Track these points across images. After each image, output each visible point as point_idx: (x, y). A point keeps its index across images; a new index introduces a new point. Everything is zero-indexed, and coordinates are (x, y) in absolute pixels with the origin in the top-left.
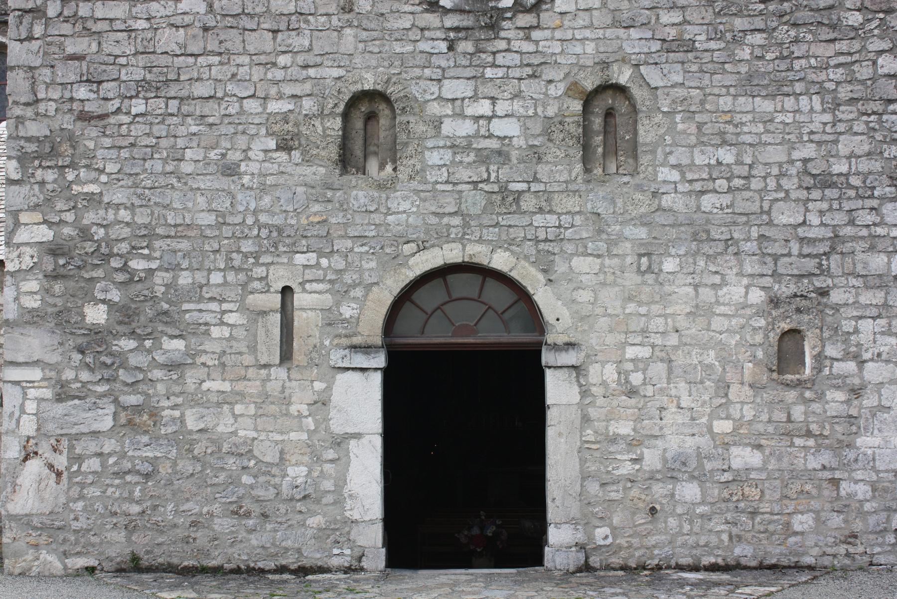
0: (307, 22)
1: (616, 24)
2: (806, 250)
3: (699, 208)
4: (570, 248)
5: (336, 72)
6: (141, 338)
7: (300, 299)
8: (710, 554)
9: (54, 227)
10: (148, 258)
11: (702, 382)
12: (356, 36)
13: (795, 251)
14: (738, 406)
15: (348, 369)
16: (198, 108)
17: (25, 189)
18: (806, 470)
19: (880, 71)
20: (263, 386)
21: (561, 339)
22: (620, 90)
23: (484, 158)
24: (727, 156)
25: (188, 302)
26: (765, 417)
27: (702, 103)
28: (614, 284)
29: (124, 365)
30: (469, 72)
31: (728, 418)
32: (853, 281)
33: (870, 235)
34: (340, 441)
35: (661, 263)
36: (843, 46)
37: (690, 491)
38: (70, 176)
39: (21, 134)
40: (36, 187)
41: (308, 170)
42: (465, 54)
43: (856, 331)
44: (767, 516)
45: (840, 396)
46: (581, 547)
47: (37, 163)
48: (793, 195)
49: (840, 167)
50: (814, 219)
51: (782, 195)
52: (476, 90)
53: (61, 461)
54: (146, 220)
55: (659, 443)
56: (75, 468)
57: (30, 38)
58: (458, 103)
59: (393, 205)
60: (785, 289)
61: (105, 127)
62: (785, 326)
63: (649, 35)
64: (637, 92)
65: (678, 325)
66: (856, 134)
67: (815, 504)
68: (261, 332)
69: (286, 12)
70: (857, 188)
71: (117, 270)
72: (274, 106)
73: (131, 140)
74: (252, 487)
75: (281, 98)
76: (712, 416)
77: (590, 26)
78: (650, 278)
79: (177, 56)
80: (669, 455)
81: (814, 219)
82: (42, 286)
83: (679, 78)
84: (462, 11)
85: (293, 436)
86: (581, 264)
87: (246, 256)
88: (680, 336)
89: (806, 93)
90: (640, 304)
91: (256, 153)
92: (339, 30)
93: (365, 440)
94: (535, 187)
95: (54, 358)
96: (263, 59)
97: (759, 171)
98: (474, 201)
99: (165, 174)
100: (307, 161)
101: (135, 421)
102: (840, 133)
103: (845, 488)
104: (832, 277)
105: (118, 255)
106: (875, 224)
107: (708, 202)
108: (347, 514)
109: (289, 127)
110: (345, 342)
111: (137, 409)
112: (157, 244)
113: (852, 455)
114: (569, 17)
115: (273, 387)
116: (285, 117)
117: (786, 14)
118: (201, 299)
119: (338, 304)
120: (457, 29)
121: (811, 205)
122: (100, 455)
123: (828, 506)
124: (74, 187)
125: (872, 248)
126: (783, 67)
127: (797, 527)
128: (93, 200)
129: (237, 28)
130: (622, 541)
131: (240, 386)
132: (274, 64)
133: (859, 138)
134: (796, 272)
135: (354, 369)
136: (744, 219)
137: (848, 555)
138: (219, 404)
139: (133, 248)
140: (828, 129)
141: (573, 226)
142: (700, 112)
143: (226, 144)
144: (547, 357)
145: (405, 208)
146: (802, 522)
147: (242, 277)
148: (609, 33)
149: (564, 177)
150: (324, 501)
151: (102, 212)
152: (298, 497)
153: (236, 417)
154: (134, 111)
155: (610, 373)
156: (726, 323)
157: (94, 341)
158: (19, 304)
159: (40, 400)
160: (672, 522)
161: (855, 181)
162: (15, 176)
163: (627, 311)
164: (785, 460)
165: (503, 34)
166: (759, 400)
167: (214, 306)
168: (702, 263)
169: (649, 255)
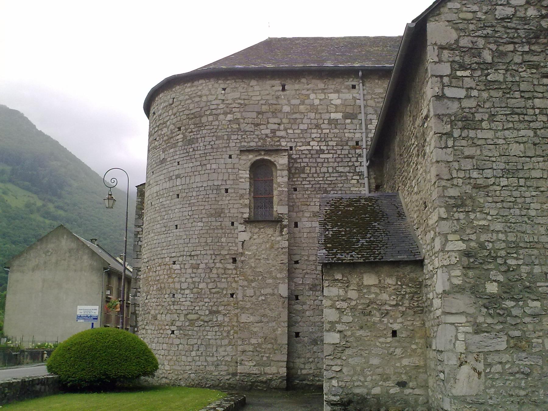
6: (517, 300)
9: (466, 242)
10: (517, 259)
16: (535, 183)
25: (540, 282)
29: (510, 315)
38: (472, 216)
40: (455, 222)
47: (455, 209)
53: (480, 367)
56: (488, 370)
57: (446, 147)
73: (502, 198)
79: (521, 157)
95: (471, 310)
101: (518, 345)
105: (500, 257)
122: (500, 363)
128: (485, 229)
139: (508, 253)
151: (490, 235)
154: (502, 184)
157: (492, 303)
158: (451, 282)
162: (445, 216)
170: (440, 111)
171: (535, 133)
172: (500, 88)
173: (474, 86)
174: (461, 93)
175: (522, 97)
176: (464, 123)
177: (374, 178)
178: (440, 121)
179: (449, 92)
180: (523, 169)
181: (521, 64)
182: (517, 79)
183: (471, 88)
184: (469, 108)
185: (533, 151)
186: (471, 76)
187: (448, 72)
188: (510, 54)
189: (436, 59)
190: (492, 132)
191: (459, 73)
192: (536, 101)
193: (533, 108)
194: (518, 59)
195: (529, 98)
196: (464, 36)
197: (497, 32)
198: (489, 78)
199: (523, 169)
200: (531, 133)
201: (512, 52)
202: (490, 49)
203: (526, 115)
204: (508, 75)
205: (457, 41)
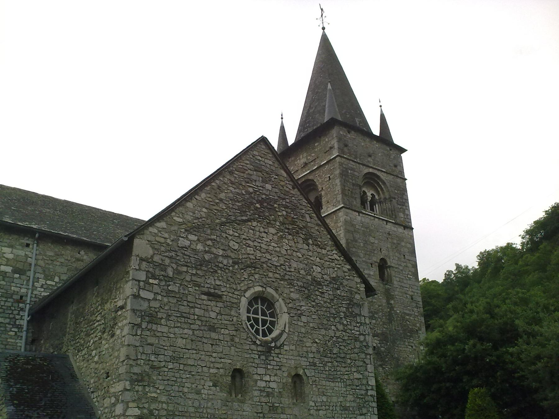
0: (221, 343)
1: (299, 356)
5: (230, 361)
16: (188, 368)
24: (325, 399)
27: (319, 382)
36: (347, 369)
40: (135, 393)
47: (136, 383)
49: (348, 405)
54: (172, 409)
57: (136, 335)
64: (304, 378)
72: (212, 371)
73: (168, 378)
83: (313, 374)
84: (262, 346)
96: (209, 354)
98: (266, 409)
100: (221, 391)
109: (216, 378)
116: (215, 375)
128: (155, 400)
132: (212, 356)
148: (297, 358)
149: (288, 403)
151: (157, 404)
161: (351, 409)
165: (272, 355)
171: (193, 332)
173: (159, 292)
174: (150, 296)
175: (188, 305)
177: (32, 332)
179: (143, 294)
182: (187, 292)
183: (157, 293)
186: (158, 285)
187: (144, 278)
188: (184, 273)
189: (137, 267)
191: (151, 281)
194: (188, 278)
195: (192, 307)
198: (169, 288)
204: (181, 288)
205: (152, 257)
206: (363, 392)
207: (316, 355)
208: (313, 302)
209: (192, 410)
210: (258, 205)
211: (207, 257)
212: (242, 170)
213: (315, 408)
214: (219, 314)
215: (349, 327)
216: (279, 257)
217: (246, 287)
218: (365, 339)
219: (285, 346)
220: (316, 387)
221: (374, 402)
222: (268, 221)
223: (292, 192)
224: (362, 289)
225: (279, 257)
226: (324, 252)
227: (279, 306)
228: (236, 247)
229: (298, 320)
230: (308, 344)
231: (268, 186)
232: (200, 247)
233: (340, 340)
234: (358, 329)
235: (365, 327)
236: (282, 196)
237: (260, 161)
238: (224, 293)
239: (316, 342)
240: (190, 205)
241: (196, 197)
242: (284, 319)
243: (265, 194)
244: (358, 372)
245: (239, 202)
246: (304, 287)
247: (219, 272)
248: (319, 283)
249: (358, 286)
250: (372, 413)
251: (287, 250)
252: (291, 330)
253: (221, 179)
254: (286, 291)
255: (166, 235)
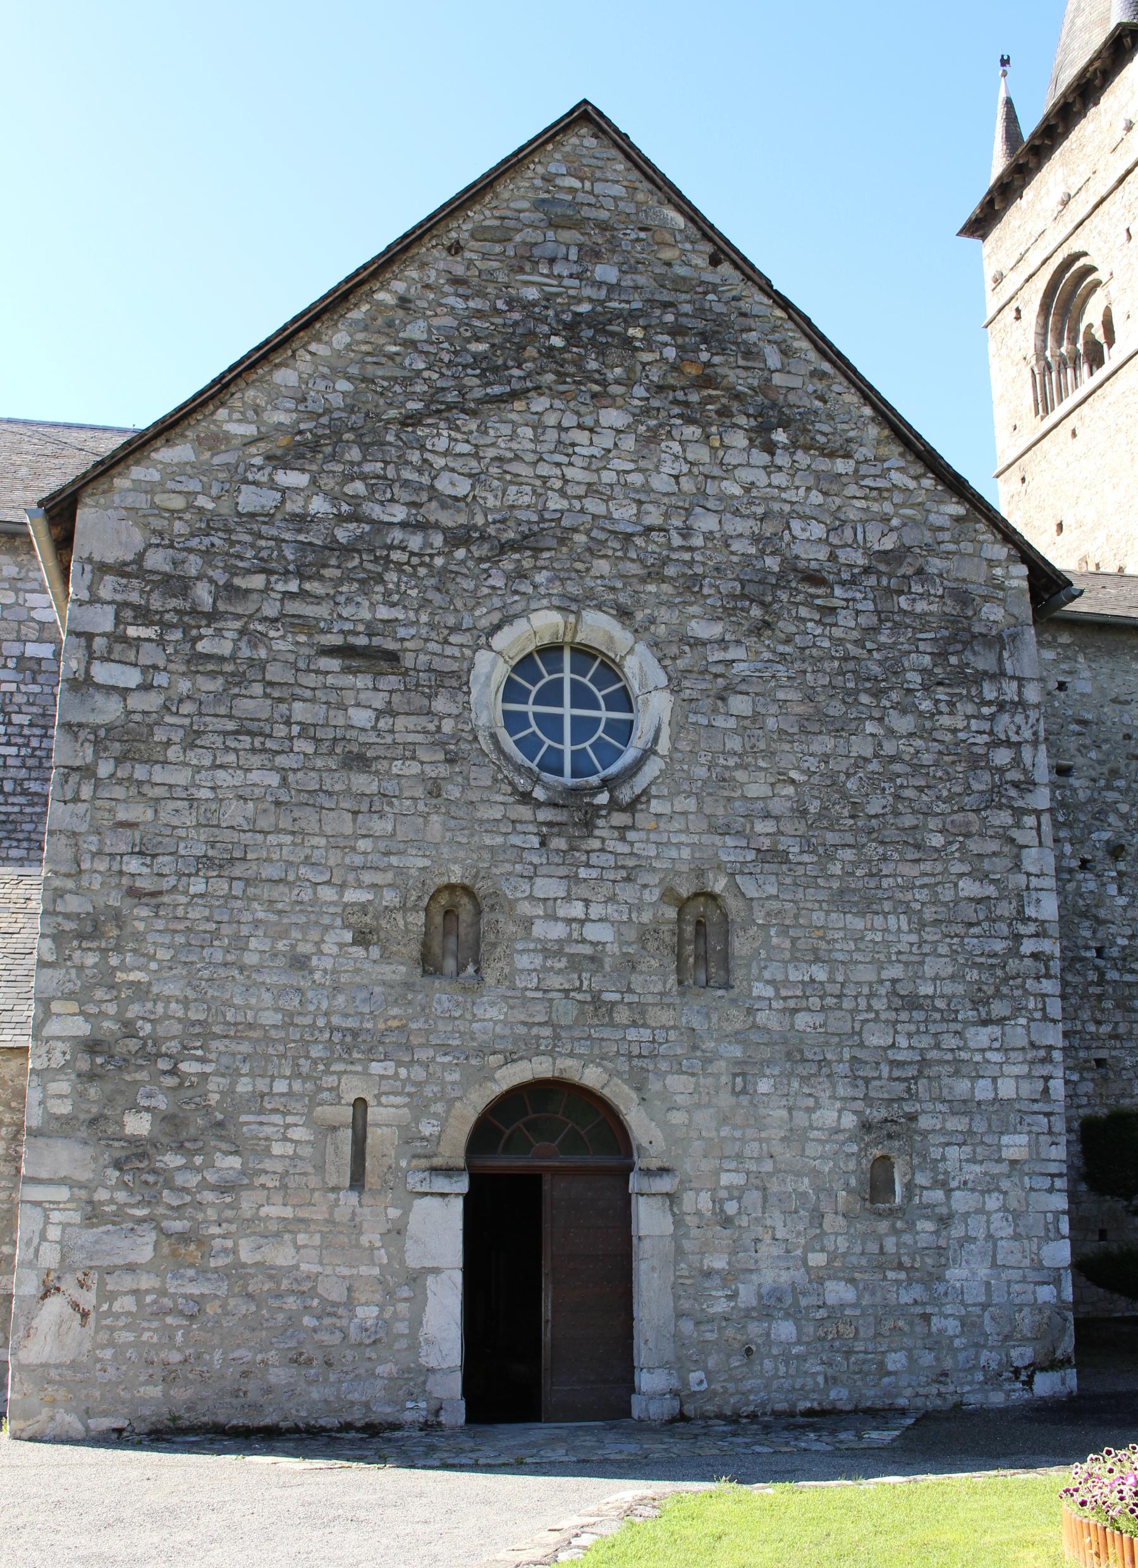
0: (391, 804)
1: (713, 829)
2: (897, 1073)
3: (792, 1026)
4: (664, 1066)
7: (374, 1113)
8: (806, 1398)
9: (92, 1020)
10: (202, 1060)
11: (796, 1212)
12: (443, 824)
13: (885, 1074)
14: (832, 1237)
15: (426, 1194)
16: (266, 892)
17: (58, 974)
18: (899, 1304)
19: (961, 894)
20: (331, 1214)
21: (654, 1164)
22: (712, 897)
23: (575, 964)
24: (820, 974)
25: (249, 1113)
26: (858, 1249)
28: (708, 1105)
29: (169, 1184)
30: (563, 871)
31: (822, 1250)
32: (940, 1107)
33: (955, 1059)
34: (416, 1278)
35: (756, 1084)
36: (927, 867)
37: (785, 1330)
38: (114, 961)
39: (58, 909)
40: (73, 972)
41: (387, 969)
42: (558, 851)
43: (944, 1158)
44: (861, 1356)
45: (928, 1226)
46: (675, 1393)
48: (883, 1016)
49: (926, 989)
50: (903, 1042)
51: (872, 1015)
52: (569, 891)
53: (88, 1299)
54: (202, 1017)
55: (754, 1277)
56: (105, 1307)
57: (76, 799)
58: (551, 903)
59: (479, 1012)
60: (877, 1114)
61: (158, 906)
62: (877, 1152)
63: (744, 843)
64: (733, 905)
65: (772, 1150)
66: (940, 956)
67: (908, 1342)
68: (330, 1149)
69: (368, 792)
70: (942, 1011)
71: (165, 1073)
72: (352, 896)
73: (188, 923)
74: (315, 1330)
75: (360, 887)
76: (808, 1249)
77: (687, 831)
78: (744, 1100)
80: (764, 1291)
81: (903, 1042)
82: (74, 1088)
84: (556, 805)
85: (364, 1270)
86: (677, 1083)
87: (315, 1062)
88: (775, 1163)
89: (895, 912)
90: (735, 1127)
91: (329, 948)
92: (425, 816)
93: (443, 1276)
94: (628, 998)
95: (84, 1175)
97: (850, 991)
98: (566, 1012)
99: (225, 965)
100: (386, 957)
102: (926, 955)
103: (936, 1323)
104: (920, 1102)
105: (166, 1055)
106: (959, 1049)
107: (802, 1020)
108: (422, 1361)
109: (368, 919)
110: (424, 1163)
111: (184, 1238)
112: (214, 1044)
113: (941, 1289)
114: (664, 819)
115: (342, 1214)
116: (363, 908)
117: (874, 830)
118: (262, 1111)
119: (417, 1120)
120: (550, 824)
121: (899, 1027)
123: (919, 1343)
124: (119, 974)
125: (956, 1073)
126: (872, 884)
127: (891, 1367)
128: (140, 991)
129: (314, 806)
130: (717, 1387)
131: (304, 1213)
132: (353, 849)
133: (944, 960)
134: (886, 1096)
135: (432, 1194)
136: (837, 1039)
137: (939, 1394)
138: (278, 1235)
139: (185, 1048)
140: (915, 949)
141: (667, 1041)
142: (794, 926)
143: (296, 934)
144: (635, 1183)
145: (491, 1014)
146: (896, 1361)
147: (309, 1086)
148: (705, 839)
149: (659, 988)
150: (397, 1346)
152: (368, 1341)
153: (298, 1248)
154: (192, 890)
155: (705, 1202)
156: (820, 1148)
157: (134, 1157)
158: (45, 1108)
159: (65, 1226)
160: (768, 1364)
161: (941, 1004)
162: (50, 958)
163: (722, 1134)
164: (879, 1294)
165: (597, 832)
166: (852, 1231)
167: (277, 1119)
168: (795, 1084)
169: (743, 1074)
170: (75, 717)
171: (284, 779)
172: (221, 673)
173: (161, 664)
174: (131, 678)
175: (266, 695)
176: (127, 746)
178: (69, 737)
179: (102, 673)
180: (244, 859)
181: (276, 620)
182: (263, 653)
183: (155, 667)
184: (144, 712)
185: (272, 819)
187: (108, 626)
189: (85, 595)
190: (188, 772)
191: (132, 632)
192: (297, 706)
193: (288, 723)
194: (271, 610)
195: (281, 700)
196: (158, 545)
197: (233, 544)
198: (201, 647)
199: (244, 859)
200: (274, 779)
201: (262, 591)
202: (211, 581)
203: (270, 736)
204: (243, 644)
205: (141, 557)
206: (999, 946)
207: (788, 827)
208: (788, 641)
209: (271, 1018)
210: (557, 341)
211: (342, 535)
212: (499, 234)
213: (777, 1005)
214: (389, 711)
215: (945, 720)
216: (640, 503)
217: (496, 618)
218: (1017, 762)
219: (654, 802)
220: (784, 930)
221: (1048, 976)
222: (596, 388)
223: (709, 276)
224: (1015, 583)
225: (640, 503)
226: (841, 466)
227: (636, 671)
228: (463, 487)
229: (715, 711)
230: (757, 789)
231: (606, 272)
232: (319, 505)
233: (898, 768)
234: (986, 726)
235: (1019, 719)
236: (666, 296)
237: (572, 190)
238: (407, 644)
239: (793, 781)
240: (285, 377)
241: (313, 347)
242: (655, 709)
243: (590, 300)
244: (983, 877)
245: (478, 340)
246: (743, 596)
247: (392, 577)
248: (814, 578)
249: (998, 571)
250: (1038, 1015)
251: (676, 477)
252: (683, 745)
253: (415, 274)
254: (664, 614)
255: (194, 486)
